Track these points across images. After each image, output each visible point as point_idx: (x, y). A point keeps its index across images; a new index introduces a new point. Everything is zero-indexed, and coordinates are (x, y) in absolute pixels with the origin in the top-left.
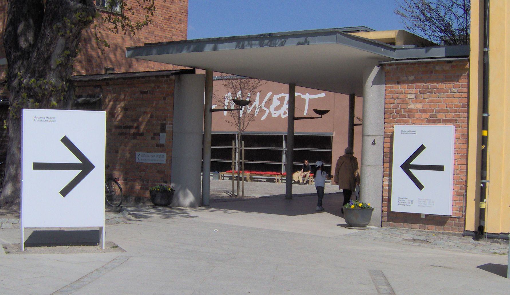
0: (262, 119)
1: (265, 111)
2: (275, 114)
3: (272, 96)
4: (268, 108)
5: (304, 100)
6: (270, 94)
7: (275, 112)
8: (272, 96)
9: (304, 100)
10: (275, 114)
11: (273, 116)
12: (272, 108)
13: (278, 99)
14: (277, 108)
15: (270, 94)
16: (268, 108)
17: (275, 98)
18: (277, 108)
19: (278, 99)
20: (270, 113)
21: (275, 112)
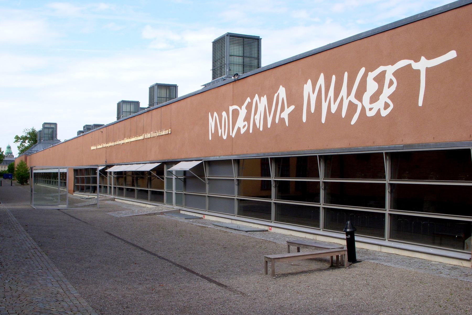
0: (353, 122)
1: (356, 106)
2: (371, 109)
3: (365, 76)
4: (361, 100)
5: (418, 72)
6: (363, 70)
7: (371, 106)
8: (365, 76)
9: (418, 72)
10: (371, 109)
11: (370, 114)
12: (366, 97)
13: (376, 79)
14: (375, 98)
15: (363, 70)
16: (361, 100)
17: (372, 75)
18: (375, 98)
19: (376, 79)
20: (363, 109)
21: (371, 106)
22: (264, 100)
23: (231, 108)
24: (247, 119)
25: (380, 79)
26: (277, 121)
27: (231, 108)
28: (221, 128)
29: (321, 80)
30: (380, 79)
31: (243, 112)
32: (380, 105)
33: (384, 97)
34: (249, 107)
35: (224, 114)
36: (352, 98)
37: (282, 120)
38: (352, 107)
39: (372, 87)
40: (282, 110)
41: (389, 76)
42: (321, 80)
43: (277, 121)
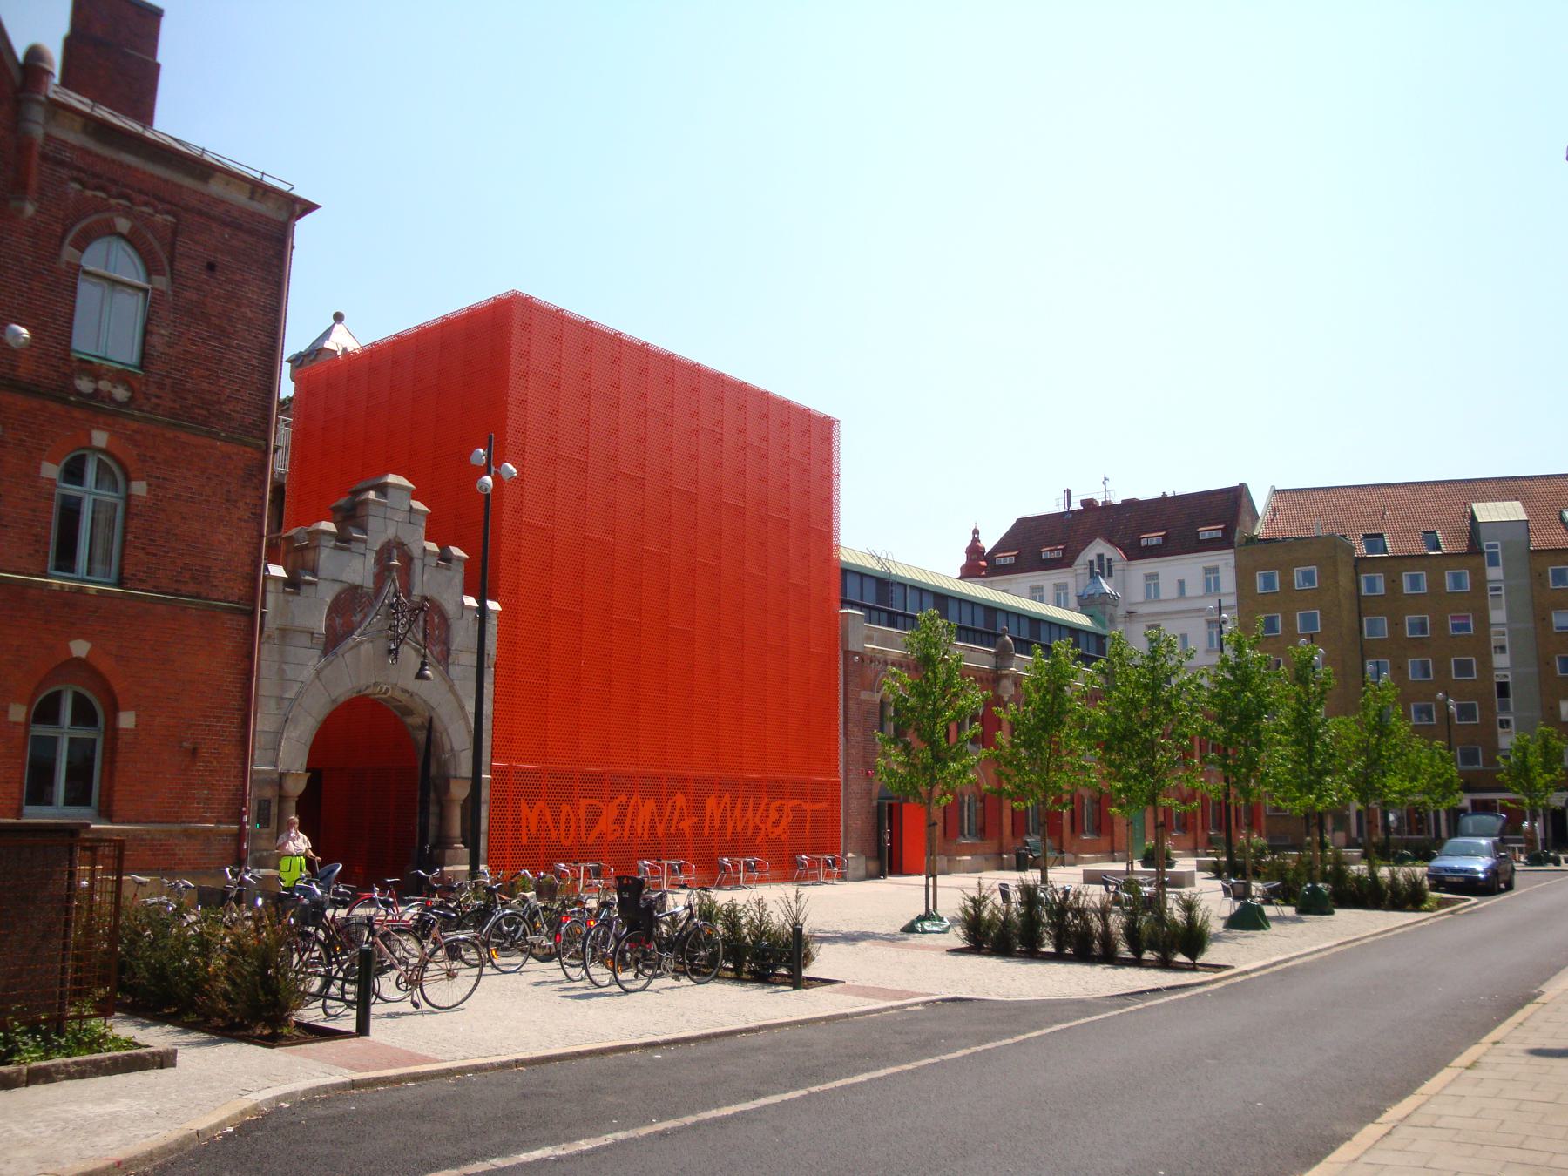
3: (768, 805)
11: (772, 836)
14: (776, 824)
17: (774, 805)
18: (776, 824)
22: (651, 804)
23: (583, 803)
24: (620, 821)
25: (779, 809)
26: (673, 830)
27: (583, 803)
28: (557, 827)
29: (727, 799)
30: (779, 809)
31: (611, 811)
32: (778, 831)
33: (784, 823)
34: (623, 808)
35: (565, 808)
36: (757, 820)
37: (680, 832)
38: (757, 829)
39: (774, 816)
40: (681, 819)
41: (786, 810)
42: (727, 799)
43: (673, 830)
